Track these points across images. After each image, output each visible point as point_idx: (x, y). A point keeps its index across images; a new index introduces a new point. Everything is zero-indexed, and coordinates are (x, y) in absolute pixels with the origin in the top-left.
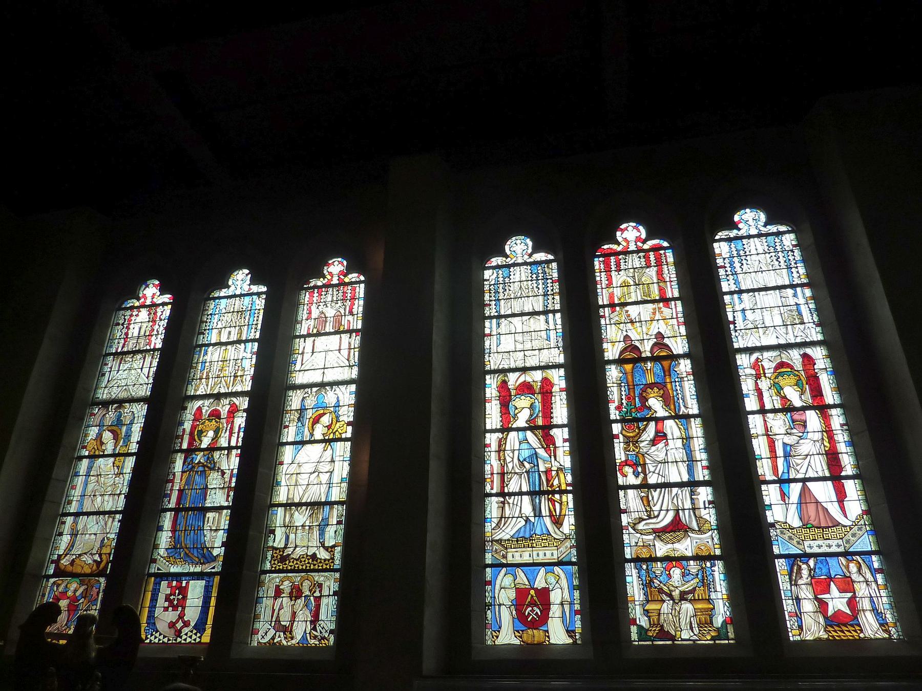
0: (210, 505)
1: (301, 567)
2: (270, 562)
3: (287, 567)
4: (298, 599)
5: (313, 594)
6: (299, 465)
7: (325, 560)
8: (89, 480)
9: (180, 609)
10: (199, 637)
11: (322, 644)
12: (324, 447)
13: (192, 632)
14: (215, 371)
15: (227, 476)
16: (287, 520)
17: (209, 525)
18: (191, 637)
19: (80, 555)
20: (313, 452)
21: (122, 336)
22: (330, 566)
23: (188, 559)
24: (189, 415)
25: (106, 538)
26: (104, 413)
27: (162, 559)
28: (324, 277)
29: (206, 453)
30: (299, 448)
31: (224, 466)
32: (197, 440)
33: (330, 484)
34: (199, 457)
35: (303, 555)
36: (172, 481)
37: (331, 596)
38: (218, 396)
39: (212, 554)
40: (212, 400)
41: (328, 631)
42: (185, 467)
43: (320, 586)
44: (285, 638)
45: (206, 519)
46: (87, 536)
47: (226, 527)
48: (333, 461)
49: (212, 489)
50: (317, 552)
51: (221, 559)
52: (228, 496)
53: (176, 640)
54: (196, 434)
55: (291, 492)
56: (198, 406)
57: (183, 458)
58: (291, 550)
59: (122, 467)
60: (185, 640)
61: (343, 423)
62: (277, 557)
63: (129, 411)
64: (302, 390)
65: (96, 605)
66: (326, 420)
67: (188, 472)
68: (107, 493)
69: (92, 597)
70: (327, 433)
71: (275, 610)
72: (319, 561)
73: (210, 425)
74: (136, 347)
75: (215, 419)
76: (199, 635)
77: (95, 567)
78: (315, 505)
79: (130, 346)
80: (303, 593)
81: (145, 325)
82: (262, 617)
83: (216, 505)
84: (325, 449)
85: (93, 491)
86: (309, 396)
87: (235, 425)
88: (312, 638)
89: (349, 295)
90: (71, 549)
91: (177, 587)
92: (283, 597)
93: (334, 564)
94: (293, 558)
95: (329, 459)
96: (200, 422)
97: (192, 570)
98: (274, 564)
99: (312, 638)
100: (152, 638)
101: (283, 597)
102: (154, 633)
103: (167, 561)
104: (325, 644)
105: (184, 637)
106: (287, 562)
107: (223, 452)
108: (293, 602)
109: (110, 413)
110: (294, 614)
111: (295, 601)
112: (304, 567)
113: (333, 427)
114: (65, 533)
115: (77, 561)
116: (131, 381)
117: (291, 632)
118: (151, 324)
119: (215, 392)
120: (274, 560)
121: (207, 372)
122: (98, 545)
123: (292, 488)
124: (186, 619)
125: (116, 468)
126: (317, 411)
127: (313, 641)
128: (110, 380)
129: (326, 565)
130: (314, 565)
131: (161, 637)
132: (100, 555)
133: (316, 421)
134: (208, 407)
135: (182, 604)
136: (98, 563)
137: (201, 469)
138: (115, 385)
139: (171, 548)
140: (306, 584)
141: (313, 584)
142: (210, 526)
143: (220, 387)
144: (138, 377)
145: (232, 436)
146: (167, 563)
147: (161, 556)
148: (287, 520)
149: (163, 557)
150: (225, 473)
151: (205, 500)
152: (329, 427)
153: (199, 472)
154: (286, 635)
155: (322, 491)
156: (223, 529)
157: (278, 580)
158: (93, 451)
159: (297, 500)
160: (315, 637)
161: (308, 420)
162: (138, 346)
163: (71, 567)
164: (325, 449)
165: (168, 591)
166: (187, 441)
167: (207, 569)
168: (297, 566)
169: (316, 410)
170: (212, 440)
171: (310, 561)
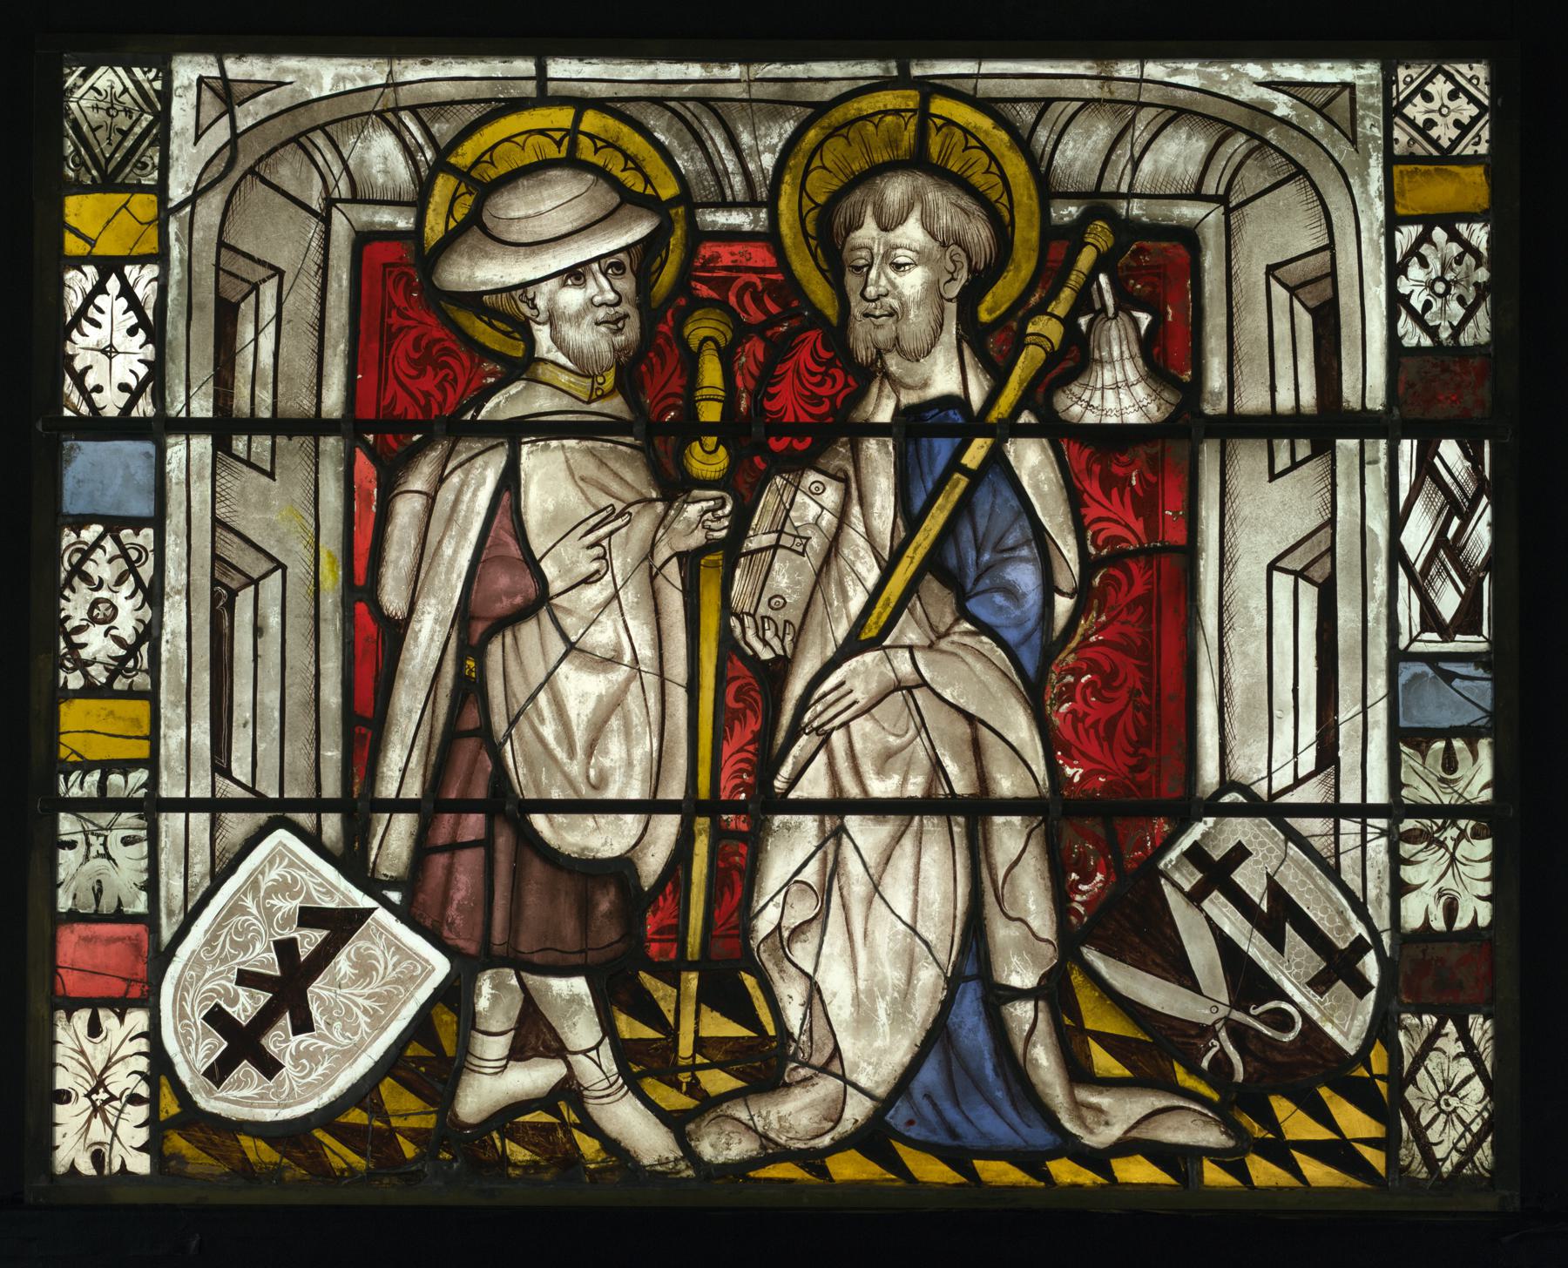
4: (796, 464)
5: (1041, 392)
11: (1280, 1151)
37: (1364, 425)
41: (1370, 966)
71: (395, 632)
80: (869, 374)
88: (1104, 1062)
92: (516, 432)
99: (1104, 1062)
101: (516, 432)
104: (1338, 1152)
141: (1026, 234)
154: (647, 1011)
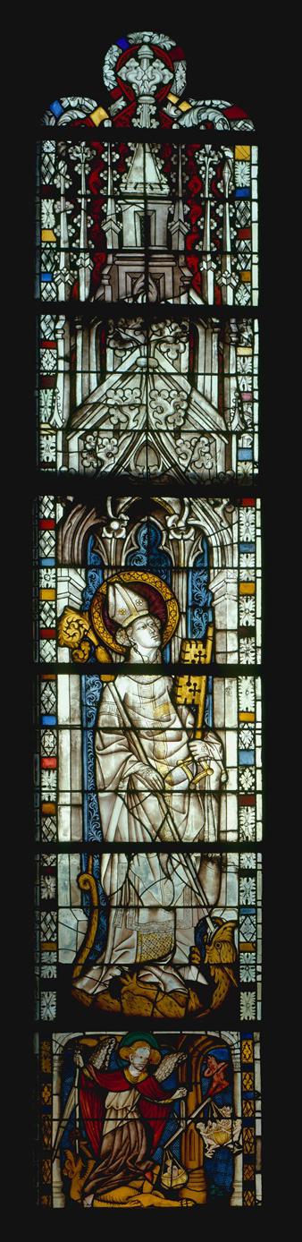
8: (98, 742)
19: (136, 968)
21: (82, 242)
25: (208, 920)
26: (91, 523)
46: (144, 913)
59: (205, 709)
63: (181, 524)
65: (233, 1105)
68: (175, 788)
69: (211, 1085)
74: (145, 289)
77: (194, 1003)
79: (122, 285)
81: (161, 211)
85: (122, 779)
90: (98, 948)
109: (115, 525)
114: (64, 898)
115: (131, 983)
116: (162, 417)
118: (183, 209)
122: (187, 939)
125: (185, 711)
128: (79, 401)
132: (204, 969)
136: (204, 992)
138: (103, 426)
144: (185, 406)
158: (85, 647)
162: (153, 288)
163: (116, 1002)
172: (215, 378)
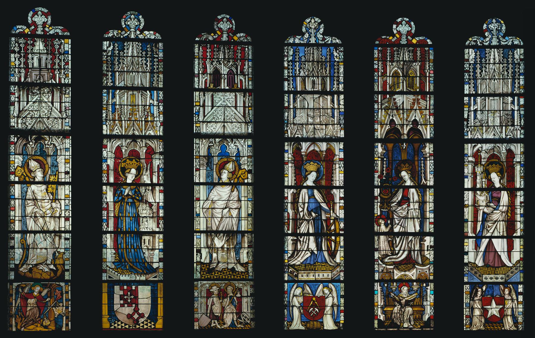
0: (144, 230)
1: (224, 277)
2: (200, 273)
3: (213, 277)
5: (235, 295)
6: (213, 202)
7: (242, 272)
8: (26, 203)
9: (134, 305)
10: (153, 325)
12: (231, 189)
13: (147, 321)
14: (126, 114)
15: (154, 208)
16: (209, 243)
17: (145, 245)
18: (147, 325)
19: (36, 265)
20: (223, 192)
21: (22, 66)
22: (246, 277)
23: (132, 270)
24: (110, 153)
26: (24, 143)
27: (111, 270)
28: (215, 33)
29: (132, 187)
30: (211, 188)
31: (151, 200)
32: (122, 175)
33: (239, 218)
34: (127, 191)
35: (225, 268)
36: (107, 209)
37: (249, 296)
38: (134, 138)
39: (153, 267)
40: (128, 141)
42: (116, 198)
43: (240, 290)
44: (219, 324)
45: (143, 241)
46: (39, 250)
47: (161, 247)
48: (239, 200)
49: (143, 217)
50: (235, 267)
51: (161, 271)
52: (158, 224)
53: (135, 327)
54: (120, 170)
55: (209, 222)
56: (116, 145)
57: (112, 190)
58: (215, 264)
59: (56, 194)
60: (143, 326)
61: (244, 170)
62: (205, 269)
63: (49, 143)
64: (207, 140)
65: (63, 303)
66: (230, 166)
67: (119, 203)
70: (232, 177)
72: (237, 273)
73: (131, 163)
74: (40, 79)
75: (135, 159)
76: (153, 323)
77: (52, 275)
78: (230, 234)
79: (33, 77)
80: (228, 294)
81: (44, 57)
82: (199, 310)
83: (149, 230)
84: (233, 190)
85: (33, 213)
86: (213, 145)
87: (154, 165)
89: (239, 55)
90: (26, 259)
91: (128, 290)
92: (213, 297)
93: (249, 275)
94: (217, 271)
95: (236, 199)
96: (121, 160)
97: (138, 278)
98: (203, 274)
100: (116, 325)
102: (116, 322)
103: (116, 272)
104: (248, 327)
105: (141, 325)
106: (213, 273)
107: (147, 188)
108: (221, 301)
109: (31, 143)
110: (223, 309)
111: (223, 299)
112: (226, 277)
113: (236, 173)
114: (16, 246)
115: (35, 269)
116: (44, 114)
117: (223, 320)
118: (50, 57)
119: (130, 133)
120: (203, 272)
121: (118, 115)
122: (50, 257)
123: (209, 219)
124: (140, 312)
125: (50, 194)
126: (221, 158)
127: (239, 326)
128: (21, 109)
129: (243, 276)
130: (234, 276)
131: (123, 325)
132: (55, 265)
133: (222, 167)
134: (126, 147)
135: (134, 301)
136: (55, 272)
137: (130, 200)
138: (28, 116)
139: (117, 262)
140: (230, 289)
142: (147, 246)
143: (134, 130)
144: (50, 111)
145: (153, 174)
146: (116, 273)
147: (109, 267)
148: (209, 243)
149: (111, 269)
150: (152, 205)
151: (139, 226)
152: (233, 173)
153: (130, 204)
155: (234, 223)
156: (159, 249)
157: (207, 286)
158: (23, 177)
159: (214, 228)
160: (241, 323)
161: (215, 166)
162: (42, 78)
164: (233, 190)
165: (121, 293)
166: (113, 176)
167: (151, 277)
168: (221, 276)
169: (220, 157)
170: (136, 176)
171: (231, 273)
172: (59, 103)
